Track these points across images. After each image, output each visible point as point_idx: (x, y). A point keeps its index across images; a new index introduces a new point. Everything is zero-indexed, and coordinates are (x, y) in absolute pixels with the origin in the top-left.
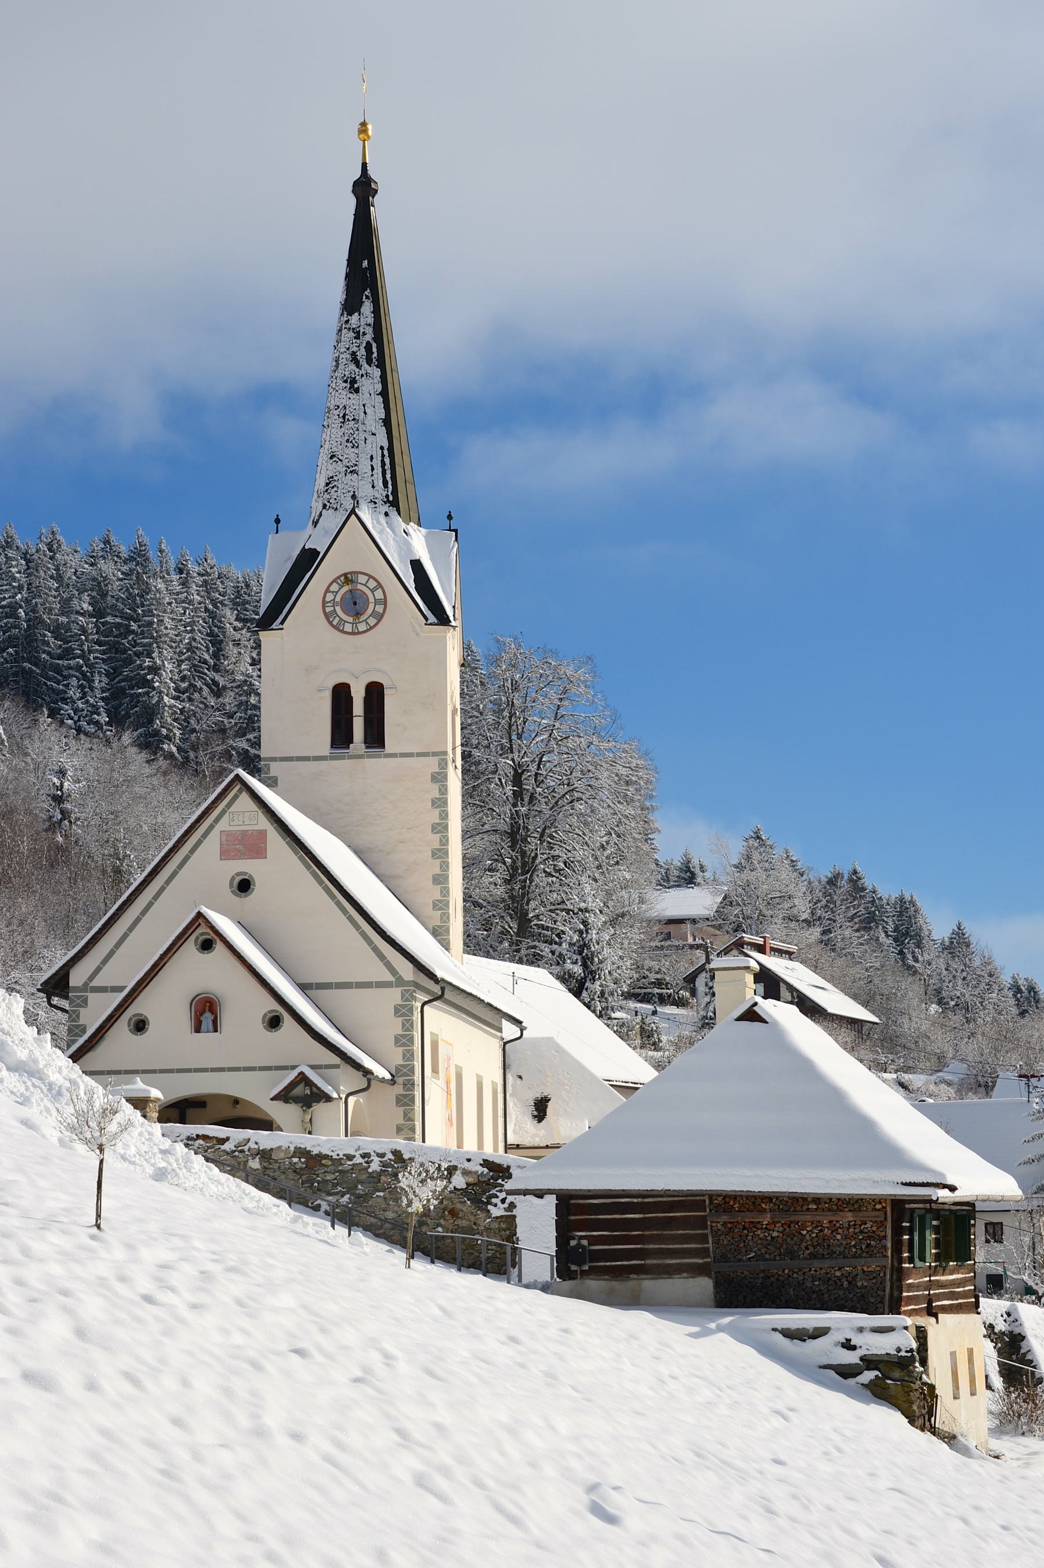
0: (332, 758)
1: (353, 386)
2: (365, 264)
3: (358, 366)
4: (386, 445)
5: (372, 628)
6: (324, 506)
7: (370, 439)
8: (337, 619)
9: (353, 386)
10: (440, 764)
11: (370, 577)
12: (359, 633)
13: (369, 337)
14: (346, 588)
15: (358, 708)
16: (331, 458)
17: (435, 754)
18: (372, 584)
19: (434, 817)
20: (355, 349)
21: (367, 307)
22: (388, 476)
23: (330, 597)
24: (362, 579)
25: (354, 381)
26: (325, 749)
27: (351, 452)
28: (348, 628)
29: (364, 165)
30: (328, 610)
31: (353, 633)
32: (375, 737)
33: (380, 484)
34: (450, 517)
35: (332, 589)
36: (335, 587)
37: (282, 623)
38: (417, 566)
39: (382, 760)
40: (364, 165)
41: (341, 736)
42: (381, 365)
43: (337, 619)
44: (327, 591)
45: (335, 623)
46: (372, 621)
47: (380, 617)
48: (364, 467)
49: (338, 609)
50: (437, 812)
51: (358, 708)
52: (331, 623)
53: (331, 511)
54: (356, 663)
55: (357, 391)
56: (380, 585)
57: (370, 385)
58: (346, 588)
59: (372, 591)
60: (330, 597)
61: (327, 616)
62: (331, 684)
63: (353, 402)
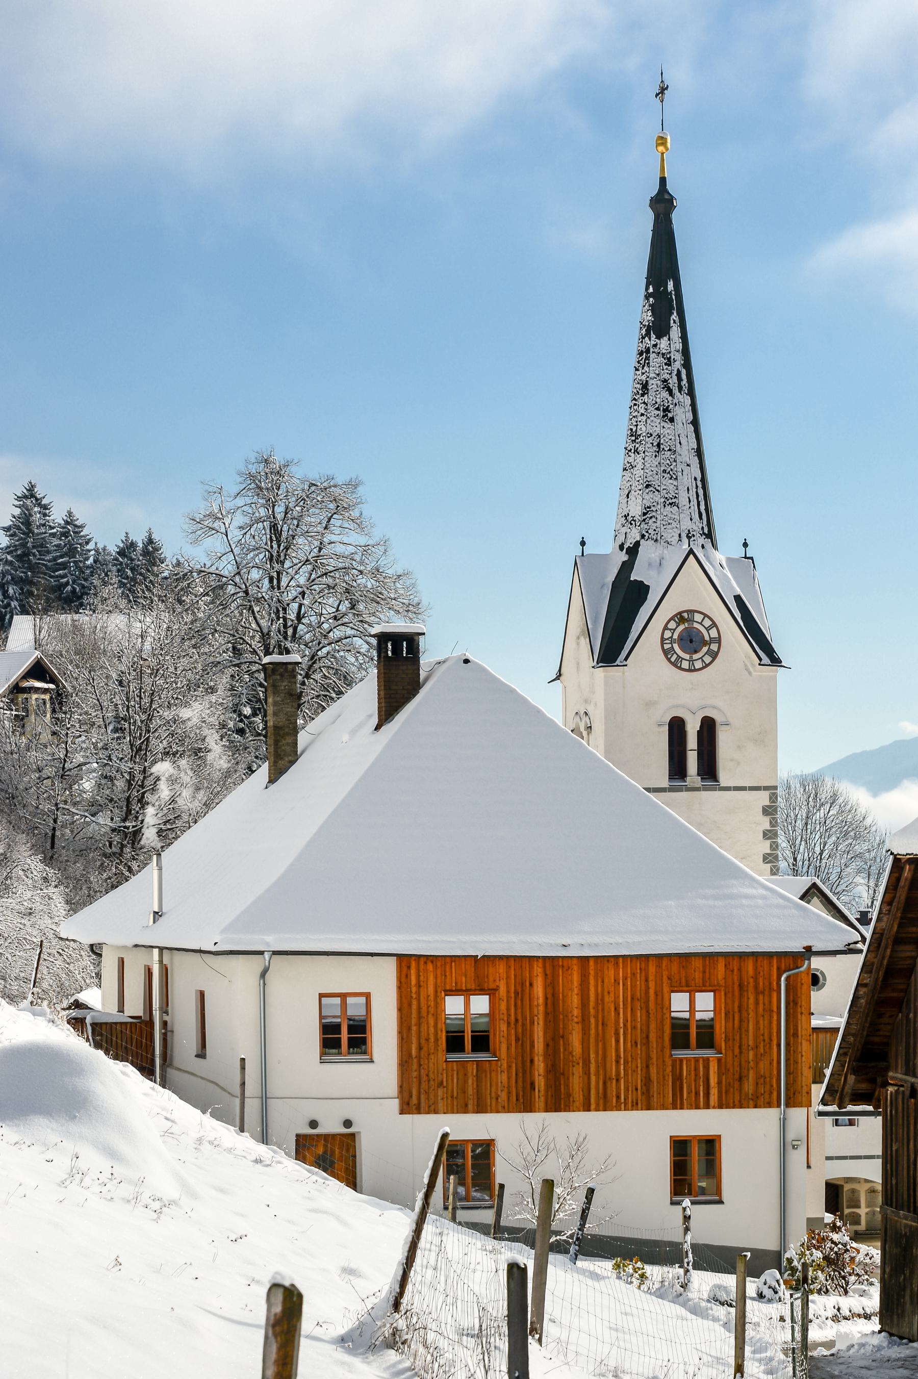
0: (672, 789)
1: (666, 414)
2: (670, 286)
3: (671, 393)
4: (699, 477)
5: (707, 665)
6: (643, 536)
7: (686, 469)
8: (675, 656)
9: (666, 414)
10: (770, 798)
11: (705, 615)
12: (696, 670)
13: (677, 365)
14: (681, 627)
15: (692, 742)
16: (647, 486)
17: (766, 788)
18: (707, 623)
19: (766, 847)
20: (667, 376)
21: (675, 332)
22: (703, 507)
23: (668, 634)
24: (698, 617)
25: (667, 410)
26: (665, 782)
27: (668, 484)
28: (685, 665)
29: (663, 180)
30: (666, 647)
31: (689, 670)
32: (709, 770)
33: (696, 516)
34: (745, 545)
35: (670, 626)
36: (672, 625)
37: (626, 659)
38: (738, 598)
39: (717, 793)
40: (663, 180)
41: (677, 769)
42: (691, 393)
43: (675, 656)
44: (666, 628)
45: (673, 660)
46: (708, 659)
47: (714, 655)
48: (683, 500)
49: (676, 646)
50: (768, 843)
51: (692, 742)
52: (669, 660)
53: (650, 542)
54: (691, 695)
55: (672, 420)
56: (714, 624)
57: (682, 414)
58: (681, 627)
59: (708, 629)
60: (668, 634)
61: (666, 652)
62: (667, 719)
63: (668, 430)
